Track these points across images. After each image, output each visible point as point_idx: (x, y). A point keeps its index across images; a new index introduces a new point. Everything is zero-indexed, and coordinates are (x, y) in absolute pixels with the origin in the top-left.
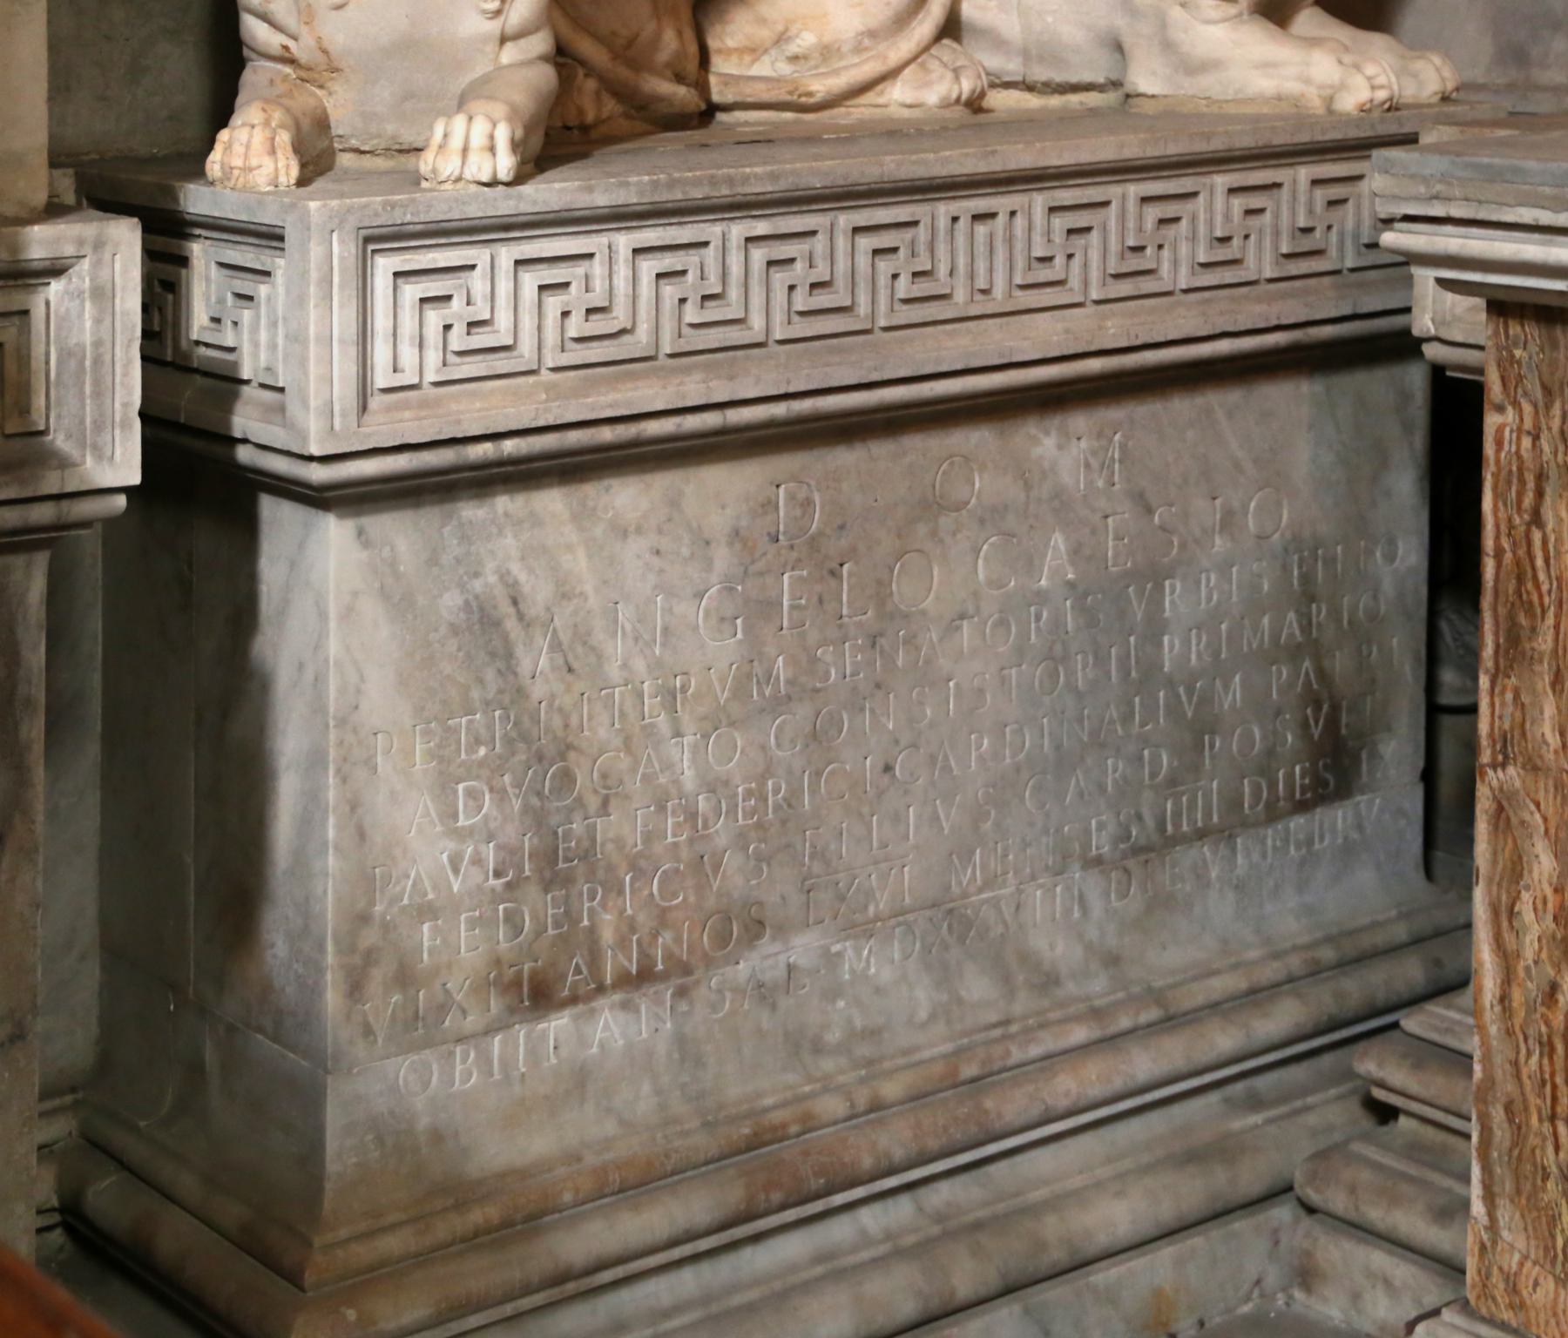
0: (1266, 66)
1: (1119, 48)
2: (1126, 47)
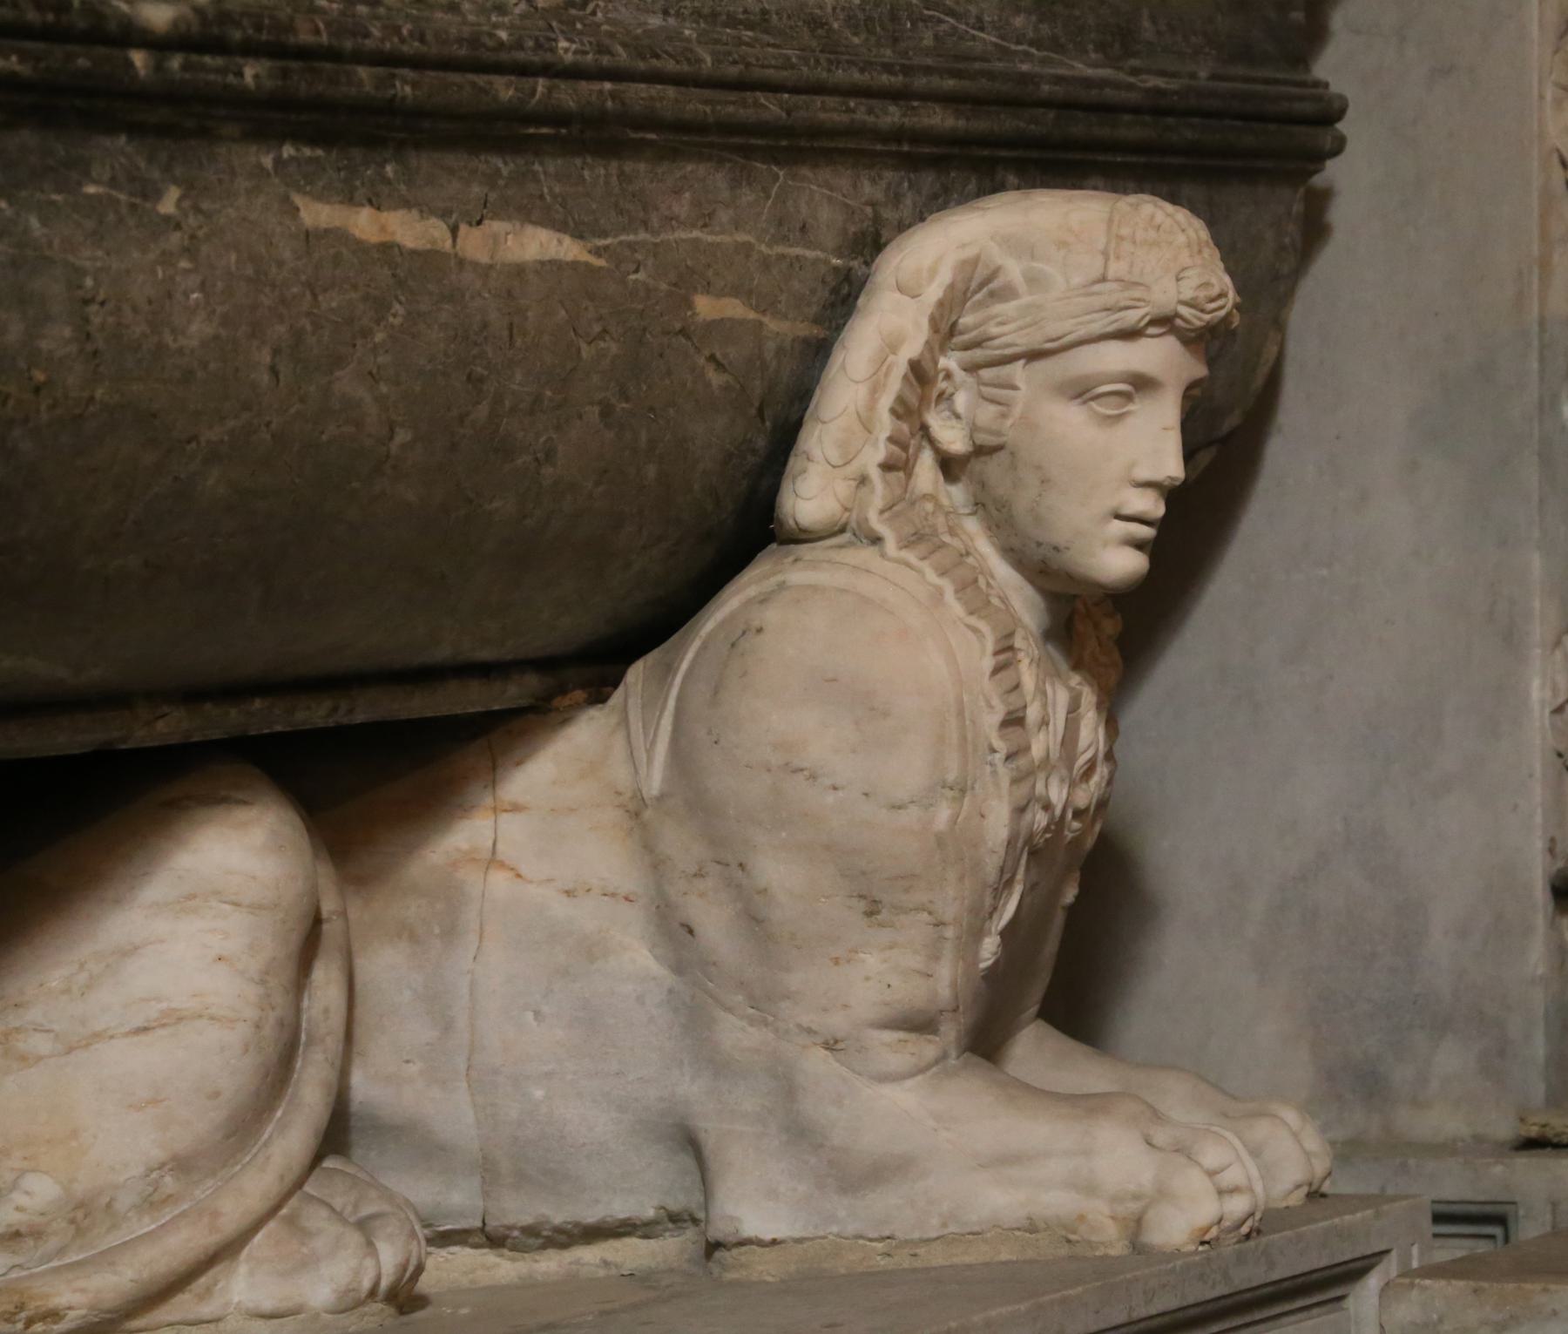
0: (1004, 1161)
1: (690, 1144)
2: (709, 1142)
